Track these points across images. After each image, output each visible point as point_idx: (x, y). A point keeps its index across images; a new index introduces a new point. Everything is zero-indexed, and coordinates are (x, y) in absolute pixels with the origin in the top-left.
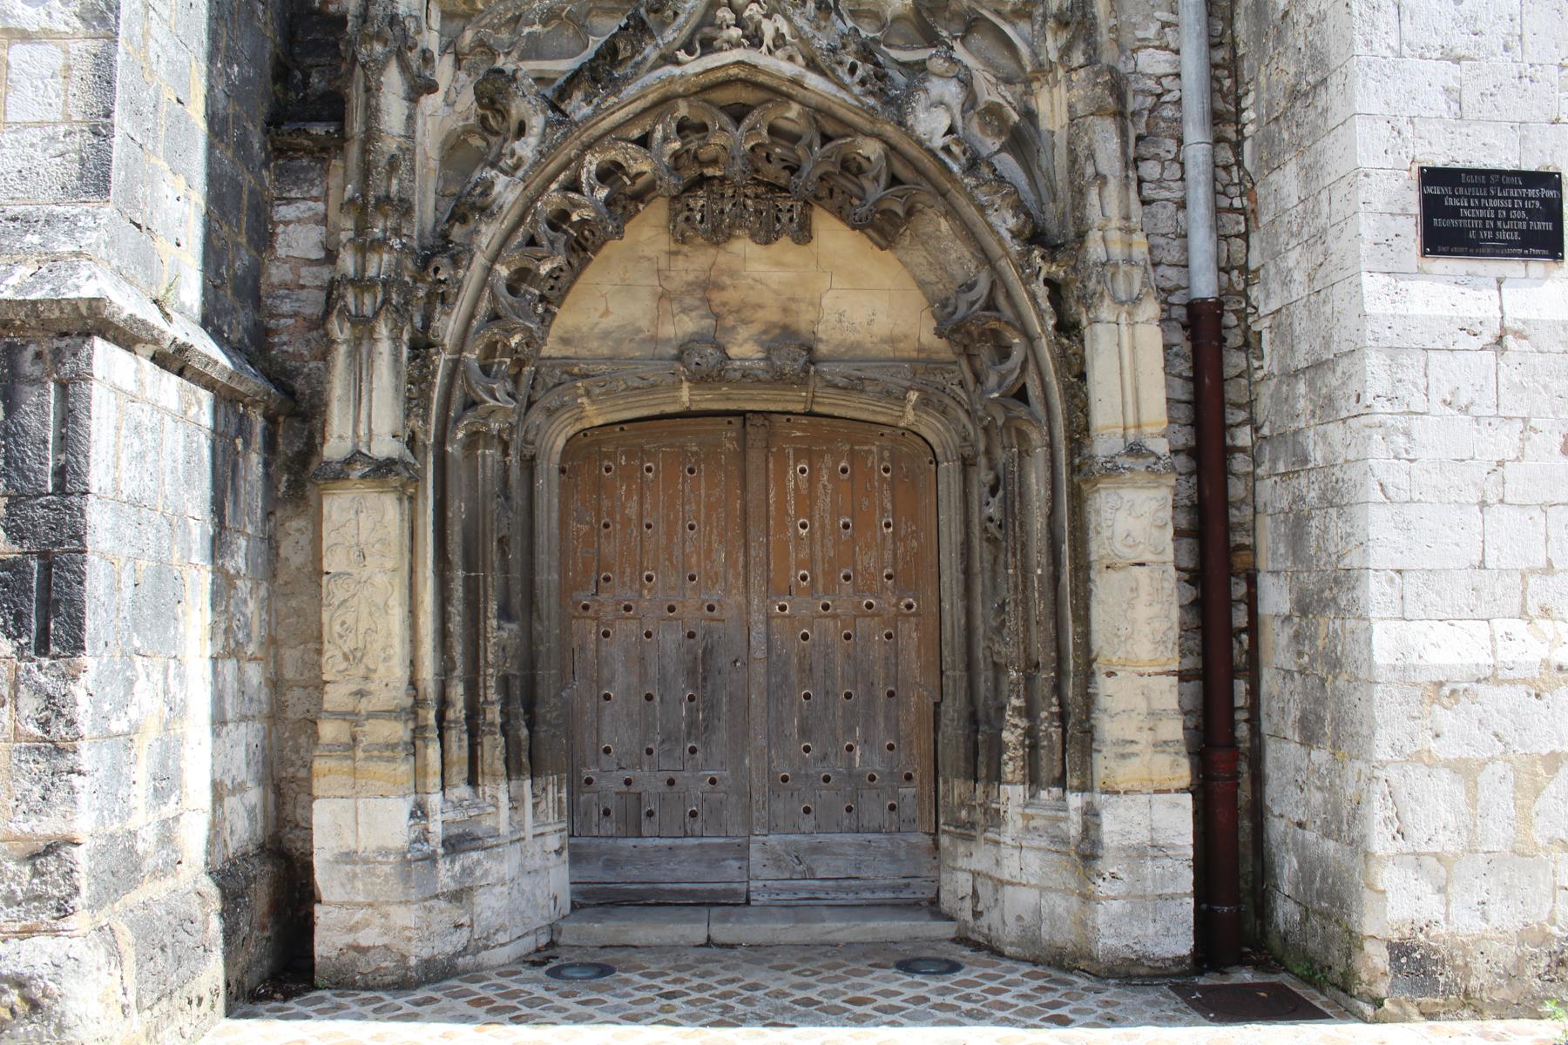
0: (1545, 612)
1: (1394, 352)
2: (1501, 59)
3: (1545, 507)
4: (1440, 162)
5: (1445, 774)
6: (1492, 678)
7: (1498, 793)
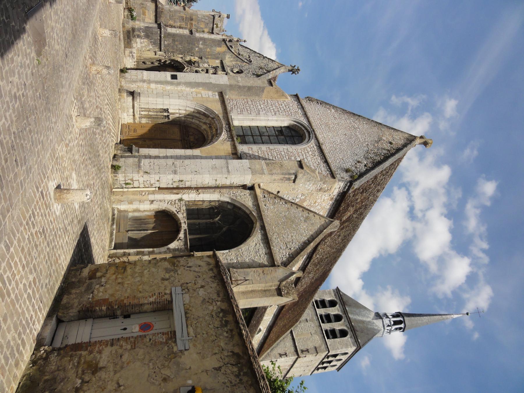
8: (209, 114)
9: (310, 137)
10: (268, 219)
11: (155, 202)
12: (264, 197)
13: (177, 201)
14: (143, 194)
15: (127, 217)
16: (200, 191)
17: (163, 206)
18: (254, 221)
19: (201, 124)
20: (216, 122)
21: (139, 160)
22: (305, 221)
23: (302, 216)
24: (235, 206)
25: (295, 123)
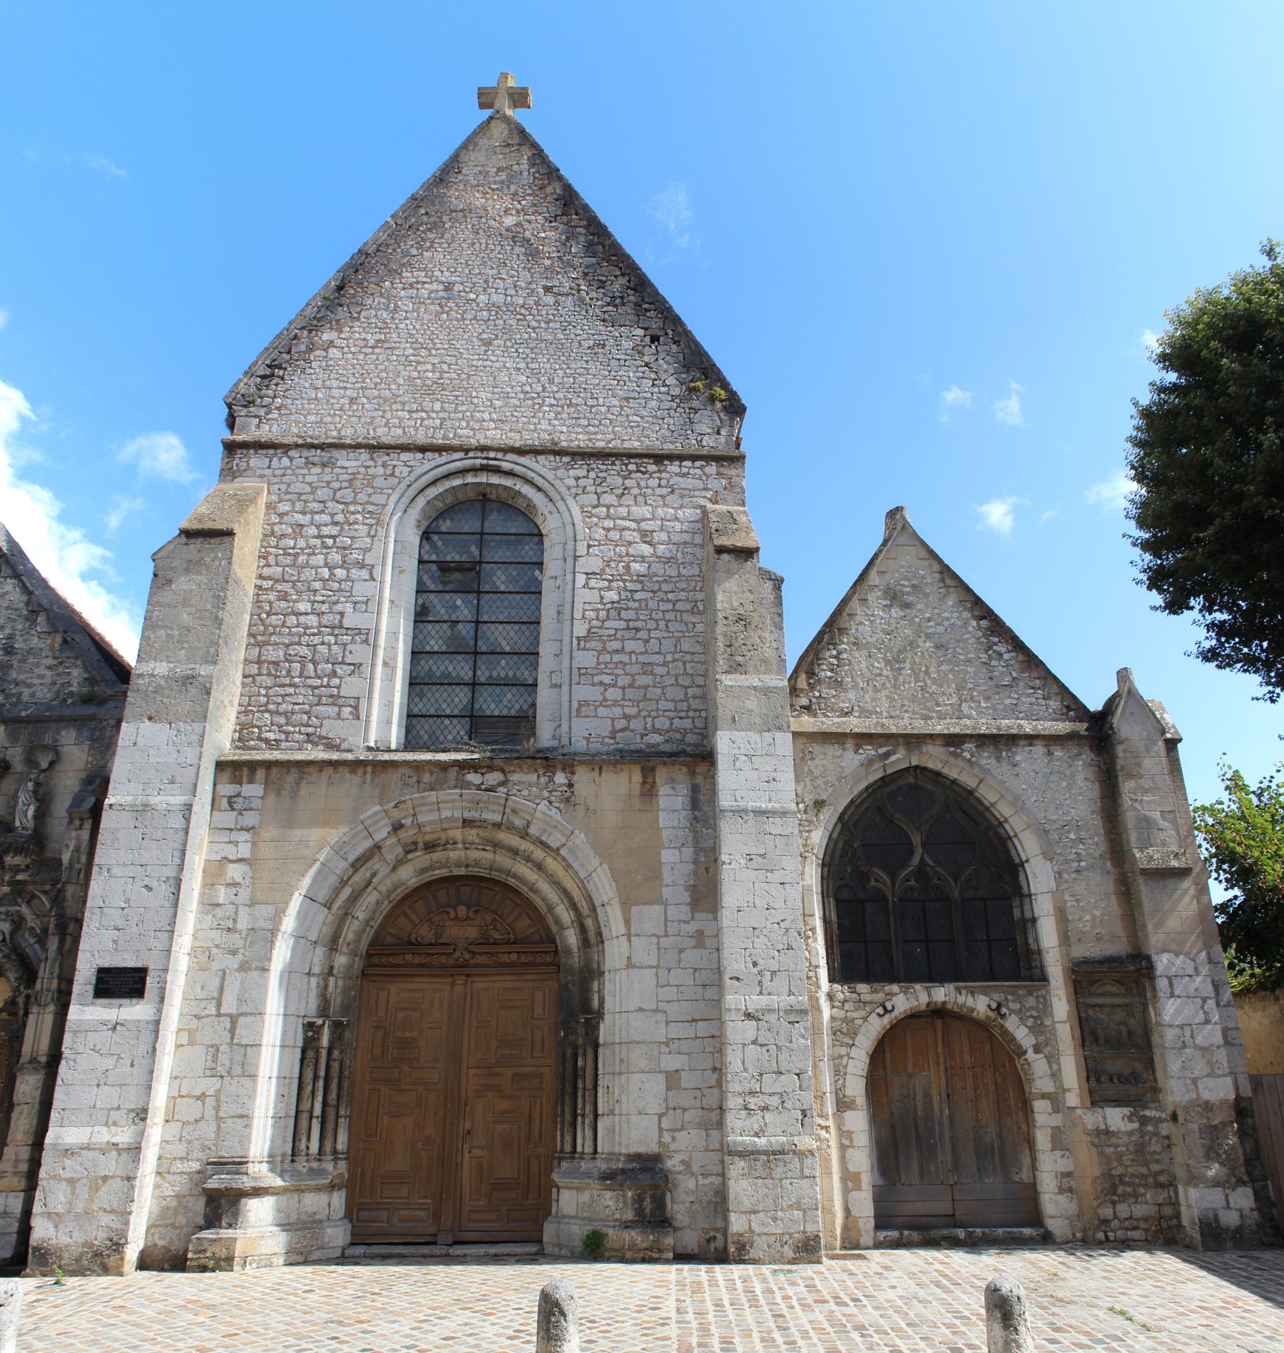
0: (115, 1124)
1: (75, 1032)
2: (135, 929)
3: (121, 1085)
4: (106, 965)
5: (64, 1183)
6: (88, 1148)
7: (83, 1191)
8: (368, 844)
11: (849, 1092)
12: (807, 708)
20: (421, 819)
21: (741, 1155)
22: (906, 606)
25: (421, 502)
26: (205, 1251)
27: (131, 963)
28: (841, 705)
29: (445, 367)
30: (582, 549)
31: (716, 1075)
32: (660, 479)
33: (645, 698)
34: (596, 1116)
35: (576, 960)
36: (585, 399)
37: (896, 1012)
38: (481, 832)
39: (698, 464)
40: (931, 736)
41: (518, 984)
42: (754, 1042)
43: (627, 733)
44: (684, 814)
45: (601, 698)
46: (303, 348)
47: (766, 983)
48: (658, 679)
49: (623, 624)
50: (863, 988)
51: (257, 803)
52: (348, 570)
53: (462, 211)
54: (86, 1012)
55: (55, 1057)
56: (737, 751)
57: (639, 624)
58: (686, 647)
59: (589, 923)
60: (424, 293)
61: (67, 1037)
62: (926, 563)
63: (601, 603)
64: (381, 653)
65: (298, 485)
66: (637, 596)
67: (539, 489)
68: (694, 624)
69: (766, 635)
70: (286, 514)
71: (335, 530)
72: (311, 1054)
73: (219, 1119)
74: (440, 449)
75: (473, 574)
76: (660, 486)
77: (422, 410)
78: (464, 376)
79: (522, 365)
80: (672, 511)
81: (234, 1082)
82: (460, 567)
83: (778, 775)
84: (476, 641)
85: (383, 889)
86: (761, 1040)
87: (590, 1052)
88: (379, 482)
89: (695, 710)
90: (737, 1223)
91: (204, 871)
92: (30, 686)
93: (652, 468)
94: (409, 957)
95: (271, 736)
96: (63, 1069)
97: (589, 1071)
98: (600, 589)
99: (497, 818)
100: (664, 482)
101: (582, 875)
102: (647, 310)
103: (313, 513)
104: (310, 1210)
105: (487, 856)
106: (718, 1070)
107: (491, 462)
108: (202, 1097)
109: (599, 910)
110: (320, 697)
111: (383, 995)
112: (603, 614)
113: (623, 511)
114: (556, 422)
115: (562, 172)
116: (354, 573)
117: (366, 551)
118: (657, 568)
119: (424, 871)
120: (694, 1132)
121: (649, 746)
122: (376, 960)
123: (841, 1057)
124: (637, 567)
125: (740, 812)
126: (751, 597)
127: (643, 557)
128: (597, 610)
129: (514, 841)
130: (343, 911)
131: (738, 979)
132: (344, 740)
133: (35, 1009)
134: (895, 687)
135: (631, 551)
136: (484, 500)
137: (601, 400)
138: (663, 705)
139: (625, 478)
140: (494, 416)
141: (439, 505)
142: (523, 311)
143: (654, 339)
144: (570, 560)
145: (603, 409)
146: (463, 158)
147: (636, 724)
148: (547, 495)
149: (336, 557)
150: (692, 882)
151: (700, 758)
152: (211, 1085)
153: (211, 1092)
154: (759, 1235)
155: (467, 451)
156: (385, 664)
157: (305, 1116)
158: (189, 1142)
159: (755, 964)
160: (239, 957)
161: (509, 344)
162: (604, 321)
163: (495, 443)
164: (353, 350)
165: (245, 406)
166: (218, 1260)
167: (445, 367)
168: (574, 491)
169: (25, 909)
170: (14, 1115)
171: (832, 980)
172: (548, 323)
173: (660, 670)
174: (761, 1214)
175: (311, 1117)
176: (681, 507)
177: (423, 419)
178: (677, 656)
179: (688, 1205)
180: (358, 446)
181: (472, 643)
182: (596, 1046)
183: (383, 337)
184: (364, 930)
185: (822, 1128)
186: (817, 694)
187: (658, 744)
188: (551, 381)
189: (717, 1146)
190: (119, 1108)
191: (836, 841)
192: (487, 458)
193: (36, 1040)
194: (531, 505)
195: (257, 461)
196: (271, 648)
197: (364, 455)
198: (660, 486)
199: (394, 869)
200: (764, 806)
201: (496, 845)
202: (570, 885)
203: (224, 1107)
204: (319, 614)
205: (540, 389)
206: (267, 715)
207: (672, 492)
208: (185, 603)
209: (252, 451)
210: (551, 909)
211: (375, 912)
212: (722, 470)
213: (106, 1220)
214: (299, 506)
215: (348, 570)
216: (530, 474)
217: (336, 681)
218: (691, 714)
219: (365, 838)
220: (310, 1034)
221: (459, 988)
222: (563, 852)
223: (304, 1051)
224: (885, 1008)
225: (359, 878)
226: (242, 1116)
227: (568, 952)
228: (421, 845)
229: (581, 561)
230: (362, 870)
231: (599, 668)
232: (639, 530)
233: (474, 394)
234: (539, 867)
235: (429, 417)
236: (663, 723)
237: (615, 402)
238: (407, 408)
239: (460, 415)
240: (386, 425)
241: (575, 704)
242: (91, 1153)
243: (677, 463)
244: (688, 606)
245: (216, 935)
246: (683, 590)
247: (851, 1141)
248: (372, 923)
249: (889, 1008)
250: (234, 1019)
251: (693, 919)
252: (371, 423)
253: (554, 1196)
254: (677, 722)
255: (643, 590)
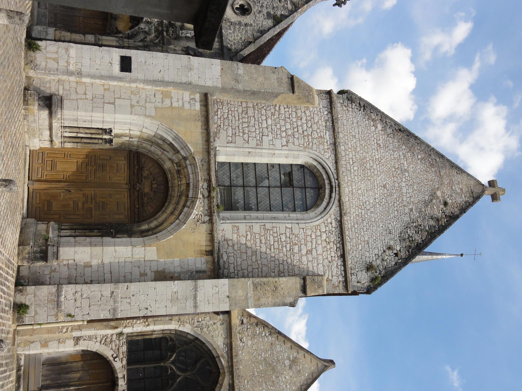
0: (76, 65)
8: (179, 148)
9: (330, 197)
10: (241, 367)
11: (81, 342)
13: (114, 337)
14: (64, 330)
15: (40, 360)
16: (150, 320)
17: (94, 347)
18: (221, 371)
19: (164, 157)
20: (189, 167)
21: (58, 290)
22: (290, 367)
23: (288, 358)
24: (197, 339)
25: (315, 163)
26: (31, 96)
27: (134, 66)
28: (244, 338)
29: (372, 171)
30: (301, 226)
31: (89, 282)
32: (334, 257)
33: (241, 253)
34: (75, 237)
35: (135, 229)
36: (366, 226)
37: (114, 363)
38: (184, 191)
39: (343, 272)
40: (233, 377)
41: (126, 208)
42: (102, 295)
43: (227, 246)
44: (194, 267)
45: (241, 235)
46: (373, 117)
47: (125, 300)
48: (250, 258)
49: (272, 243)
50: (124, 348)
51: (193, 108)
52: (285, 137)
53: (440, 175)
54: (116, 54)
55: (101, 46)
56: (220, 287)
57: (272, 250)
58: (264, 268)
59: (150, 233)
60: (402, 161)
61: (107, 48)
62: (311, 377)
63: (280, 234)
64: (253, 150)
65: (317, 117)
66: (284, 249)
67: (325, 209)
68: (274, 272)
69: (270, 299)
70: (305, 114)
71: (301, 131)
72: (100, 131)
73: (77, 100)
74: (337, 169)
75: (289, 185)
76: (332, 257)
77: (353, 163)
78: (369, 178)
79: (377, 201)
80: (321, 262)
81: (91, 104)
82: (291, 180)
83: (211, 305)
84: (262, 187)
85: (162, 156)
86: (102, 298)
87: (99, 234)
88: (321, 147)
89: (238, 273)
90: (30, 289)
91: (167, 91)
92: (234, 32)
93: (339, 254)
94: (137, 167)
95: (219, 112)
96: (97, 47)
97: (92, 234)
98: (285, 233)
99: (190, 195)
100: (334, 258)
101: (169, 229)
102: (408, 251)
103: (307, 123)
104: (43, 133)
105: (176, 194)
106: (91, 282)
107: (334, 189)
108: (85, 94)
109: (155, 235)
110: (235, 129)
111: (123, 159)
112: (275, 235)
113: (319, 242)
114: (354, 215)
115: (464, 214)
116: (284, 140)
117: (294, 144)
118: (297, 257)
119: (170, 171)
120: (67, 273)
121: (222, 255)
122: (136, 155)
123: (96, 339)
124: (296, 248)
125: (196, 289)
126: (286, 293)
127: (301, 250)
128: (277, 233)
129: (182, 203)
130: (153, 141)
131: (127, 289)
132: (219, 138)
133: (117, 39)
134: (254, 362)
135: (303, 246)
136: (319, 188)
137: (366, 233)
138: (239, 260)
139: (333, 242)
140: (354, 190)
141: (315, 171)
142: (400, 200)
143: (396, 255)
144: (297, 222)
145: (362, 234)
146: (464, 175)
147: (230, 249)
148: (323, 212)
149: (290, 132)
150: (166, 271)
151: (216, 271)
152: (89, 96)
153: (87, 96)
154: (25, 298)
155: (337, 179)
156: (249, 152)
157: (77, 130)
158: (69, 90)
159: (133, 295)
160: (136, 104)
161: (386, 195)
162: (401, 233)
163: (342, 191)
164: (375, 136)
165: (347, 97)
166: (27, 101)
167: (372, 171)
168: (326, 222)
169: (153, 35)
170: (81, 35)
171: (129, 336)
172: (397, 210)
173: (254, 258)
174: (33, 299)
175: (77, 133)
176: (324, 266)
177: (349, 163)
178: (260, 265)
179: (39, 271)
180: (335, 139)
181: (260, 185)
182: (102, 236)
183: (382, 146)
184: (147, 150)
185: (67, 329)
186: (249, 327)
187: (223, 258)
188: (372, 212)
189: (61, 283)
190: (82, 66)
191: (186, 337)
192: (336, 188)
193: (106, 40)
194: (318, 206)
195: (325, 102)
196: (253, 111)
197: (332, 141)
198: (332, 257)
199: (170, 159)
200: (198, 299)
201: (180, 197)
202: (165, 225)
203: (82, 101)
204: (267, 128)
205: (368, 208)
206: (227, 111)
207: (330, 262)
208: (266, 78)
209: (329, 100)
210: (156, 219)
211: (154, 153)
212: (341, 283)
213: (43, 64)
214: (309, 118)
215: (285, 137)
216: (331, 205)
217: (241, 134)
218: (236, 272)
219: (181, 147)
220: (108, 131)
221: (125, 186)
222: (177, 221)
223: (101, 129)
224: (116, 357)
225: (166, 147)
226: (78, 108)
227: (139, 226)
228: (179, 168)
229: (297, 225)
230: (169, 147)
231: (253, 234)
232: (312, 249)
233: (362, 182)
234: (172, 213)
235: (350, 165)
236: (232, 260)
237: (366, 239)
238: (354, 157)
239: (353, 177)
240: (346, 149)
241: (237, 225)
242: (67, 57)
243: (342, 264)
244: (282, 270)
245: (144, 96)
246: (288, 267)
247: (61, 343)
248: (149, 153)
249: (116, 360)
250: (113, 103)
251: (151, 272)
252: (345, 144)
253: (44, 222)
254: (232, 266)
255: (287, 251)
